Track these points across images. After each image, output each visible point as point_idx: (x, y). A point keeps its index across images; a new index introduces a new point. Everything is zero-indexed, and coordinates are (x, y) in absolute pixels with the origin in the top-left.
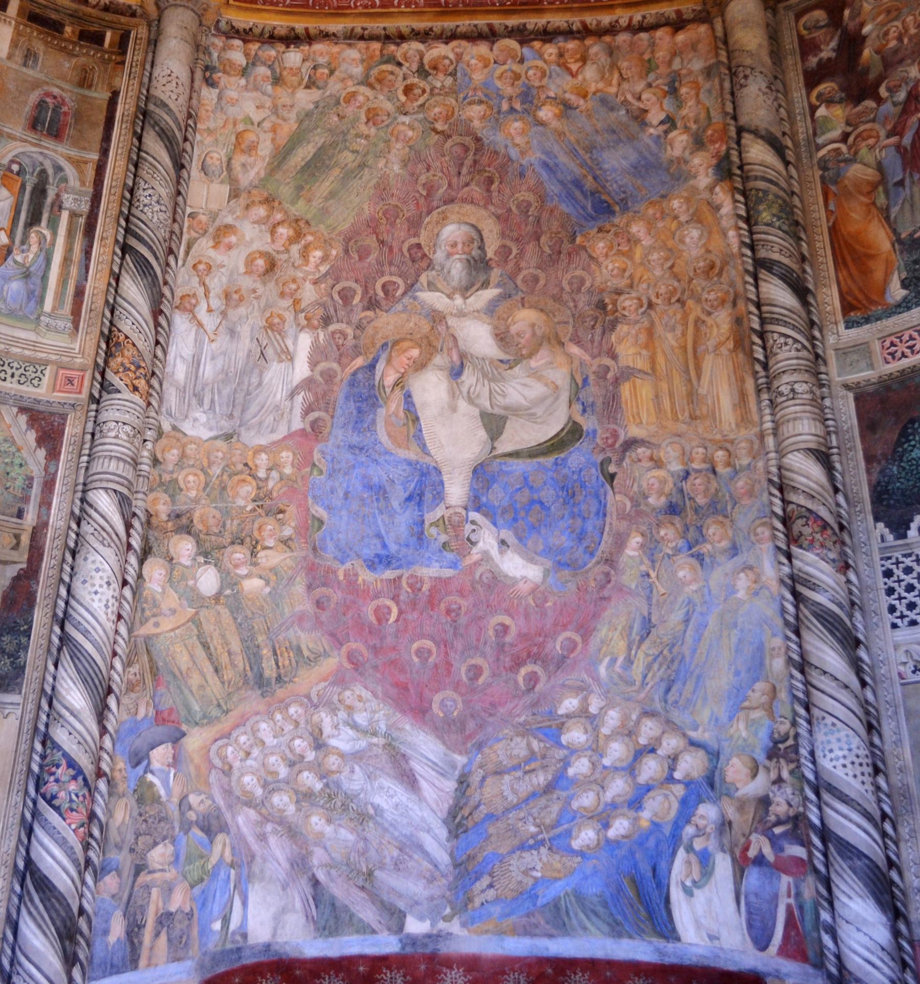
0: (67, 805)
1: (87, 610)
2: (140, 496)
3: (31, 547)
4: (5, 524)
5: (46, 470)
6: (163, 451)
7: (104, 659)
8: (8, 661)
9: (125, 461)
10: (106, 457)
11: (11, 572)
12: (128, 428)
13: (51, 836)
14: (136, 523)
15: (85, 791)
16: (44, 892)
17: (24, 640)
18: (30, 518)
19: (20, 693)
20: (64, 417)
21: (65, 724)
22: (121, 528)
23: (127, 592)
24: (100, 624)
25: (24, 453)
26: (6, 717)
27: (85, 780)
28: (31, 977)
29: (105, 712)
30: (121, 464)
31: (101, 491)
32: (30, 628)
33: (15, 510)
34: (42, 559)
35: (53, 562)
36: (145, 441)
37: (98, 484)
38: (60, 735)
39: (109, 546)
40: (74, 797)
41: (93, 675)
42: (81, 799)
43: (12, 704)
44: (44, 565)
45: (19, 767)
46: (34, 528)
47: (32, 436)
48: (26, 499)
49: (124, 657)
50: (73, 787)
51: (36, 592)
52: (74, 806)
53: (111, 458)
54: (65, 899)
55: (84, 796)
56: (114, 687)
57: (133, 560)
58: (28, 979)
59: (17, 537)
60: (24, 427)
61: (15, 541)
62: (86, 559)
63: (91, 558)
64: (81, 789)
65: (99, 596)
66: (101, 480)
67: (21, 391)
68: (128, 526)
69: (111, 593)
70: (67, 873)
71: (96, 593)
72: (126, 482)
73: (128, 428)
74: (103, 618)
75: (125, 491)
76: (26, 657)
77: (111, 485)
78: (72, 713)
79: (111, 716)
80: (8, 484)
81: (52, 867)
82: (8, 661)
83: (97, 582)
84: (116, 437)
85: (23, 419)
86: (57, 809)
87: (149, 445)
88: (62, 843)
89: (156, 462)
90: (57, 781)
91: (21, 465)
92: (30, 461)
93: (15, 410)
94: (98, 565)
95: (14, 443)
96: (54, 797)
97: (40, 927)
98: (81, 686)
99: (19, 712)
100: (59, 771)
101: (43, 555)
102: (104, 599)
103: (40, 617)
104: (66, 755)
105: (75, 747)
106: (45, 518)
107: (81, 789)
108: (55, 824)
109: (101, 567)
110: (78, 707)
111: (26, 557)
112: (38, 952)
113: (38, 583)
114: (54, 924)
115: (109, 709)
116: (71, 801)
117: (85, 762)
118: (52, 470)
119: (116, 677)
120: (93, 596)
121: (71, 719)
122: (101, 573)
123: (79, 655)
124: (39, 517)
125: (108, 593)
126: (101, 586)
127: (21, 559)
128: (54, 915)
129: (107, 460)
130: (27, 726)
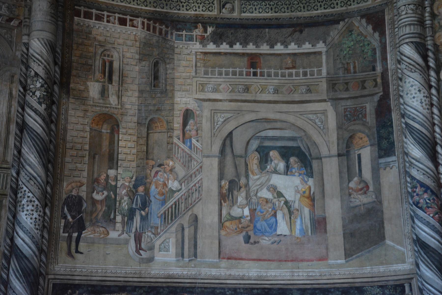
0: (425, 206)
1: (412, 107)
2: (428, 38)
3: (383, 83)
4: (368, 76)
5: (381, 42)
6: (438, 9)
7: (427, 129)
8: (386, 141)
9: (414, 25)
10: (403, 26)
11: (376, 98)
12: (411, 6)
13: (421, 222)
14: (430, 54)
15: (434, 197)
16: (425, 249)
17: (390, 129)
18: (379, 69)
19: (395, 155)
20: (383, 12)
21: (415, 166)
22: (419, 60)
23: (434, 91)
24: (420, 113)
25: (369, 38)
26: (391, 169)
27: (432, 191)
28: (430, 290)
29: (437, 155)
30: (412, 27)
31: (405, 45)
32: (392, 123)
33: (371, 68)
34: (389, 88)
35: (395, 87)
36: (425, 7)
37: (403, 42)
38: (414, 173)
39: (415, 71)
40: (428, 201)
41: (423, 139)
42: (432, 201)
43: (392, 161)
44: (391, 90)
45: (403, 191)
46: (382, 73)
47: (370, 28)
48: (375, 61)
49: (439, 124)
50: (426, 196)
51: (390, 104)
52: (429, 205)
53: (406, 26)
54: (437, 251)
55: (433, 199)
56: (438, 141)
57: (432, 73)
58: (429, 292)
59: (375, 80)
60: (365, 24)
61: (374, 83)
62: (405, 82)
63: (407, 81)
64: (431, 196)
65: (416, 99)
66: (403, 39)
67: (359, 7)
68: (425, 58)
69: (422, 95)
70: (434, 238)
71: (414, 98)
72: (417, 35)
73: (411, 6)
74: (420, 109)
75: (418, 40)
76: (393, 137)
77: (407, 40)
78: (416, 161)
79: (440, 156)
80: (365, 56)
81: (426, 237)
82: (386, 141)
83: (413, 92)
84: (406, 13)
85: (364, 21)
86: (421, 208)
87: (428, 9)
88: (428, 224)
89: (433, 16)
90: (417, 195)
91: (368, 44)
92: (372, 41)
93: (359, 18)
94: (412, 83)
95: (362, 34)
96: (418, 203)
97: (427, 266)
98: (418, 146)
99: (397, 165)
100: (417, 190)
101: (389, 85)
102: (419, 99)
103: (394, 116)
104: (418, 181)
105: (422, 177)
106: (386, 66)
107: (431, 196)
108: (422, 216)
109: (413, 84)
110: (418, 157)
111: (381, 89)
112: (430, 278)
113: (390, 99)
114: (434, 264)
115: (438, 153)
116: (427, 203)
117: (428, 182)
118: (383, 41)
119: (438, 136)
120: (413, 100)
121: (417, 163)
122: (414, 87)
123: (413, 131)
124: (383, 67)
125: (420, 96)
126: (416, 93)
127: (380, 90)
128: (433, 260)
129: (404, 28)
130: (402, 171)
